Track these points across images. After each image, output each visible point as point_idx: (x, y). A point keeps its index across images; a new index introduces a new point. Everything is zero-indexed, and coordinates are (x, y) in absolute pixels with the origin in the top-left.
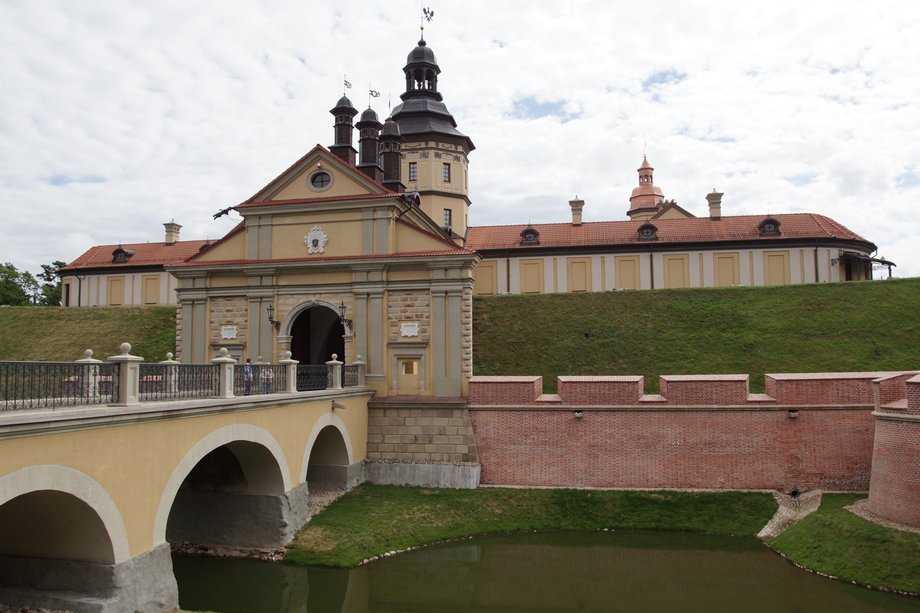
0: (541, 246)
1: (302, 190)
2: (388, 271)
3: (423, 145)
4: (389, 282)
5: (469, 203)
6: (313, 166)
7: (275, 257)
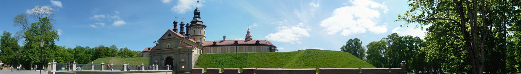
1: (167, 37)
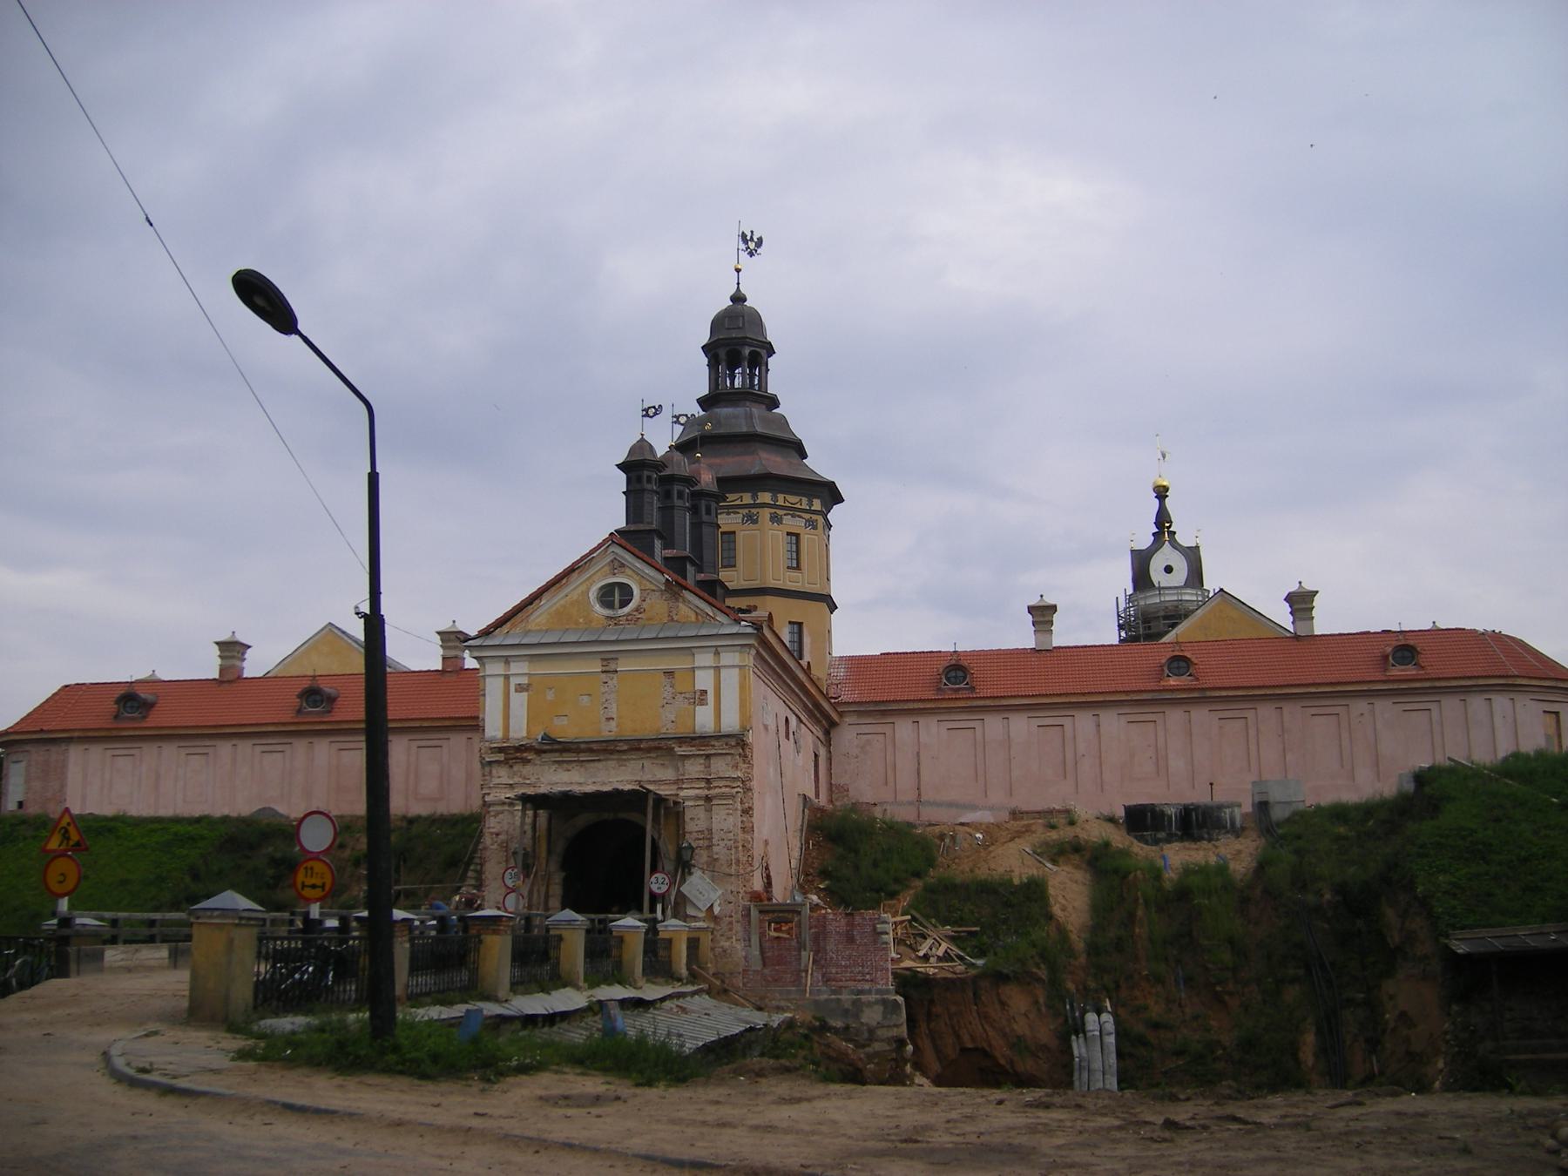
3: (747, 499)
5: (833, 607)
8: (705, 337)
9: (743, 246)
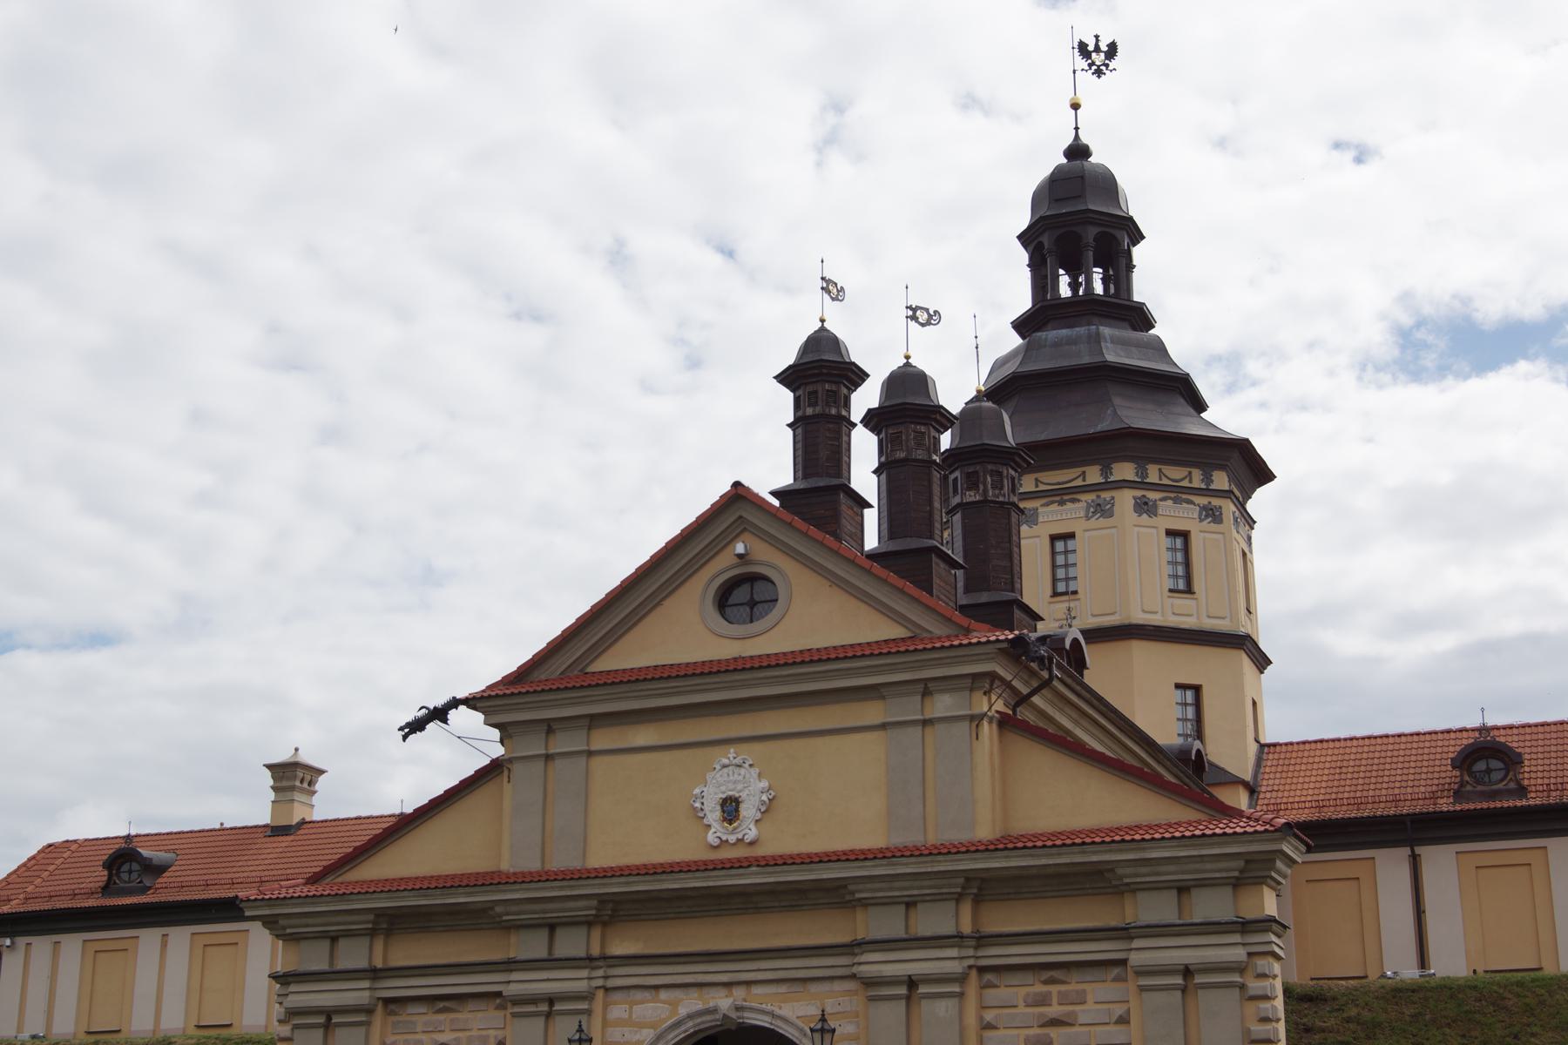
0: (1534, 800)
1: (687, 634)
2: (978, 901)
3: (1094, 475)
4: (982, 940)
5: (1262, 662)
6: (723, 554)
7: (597, 860)
8: (1023, 220)
9: (1084, 64)
